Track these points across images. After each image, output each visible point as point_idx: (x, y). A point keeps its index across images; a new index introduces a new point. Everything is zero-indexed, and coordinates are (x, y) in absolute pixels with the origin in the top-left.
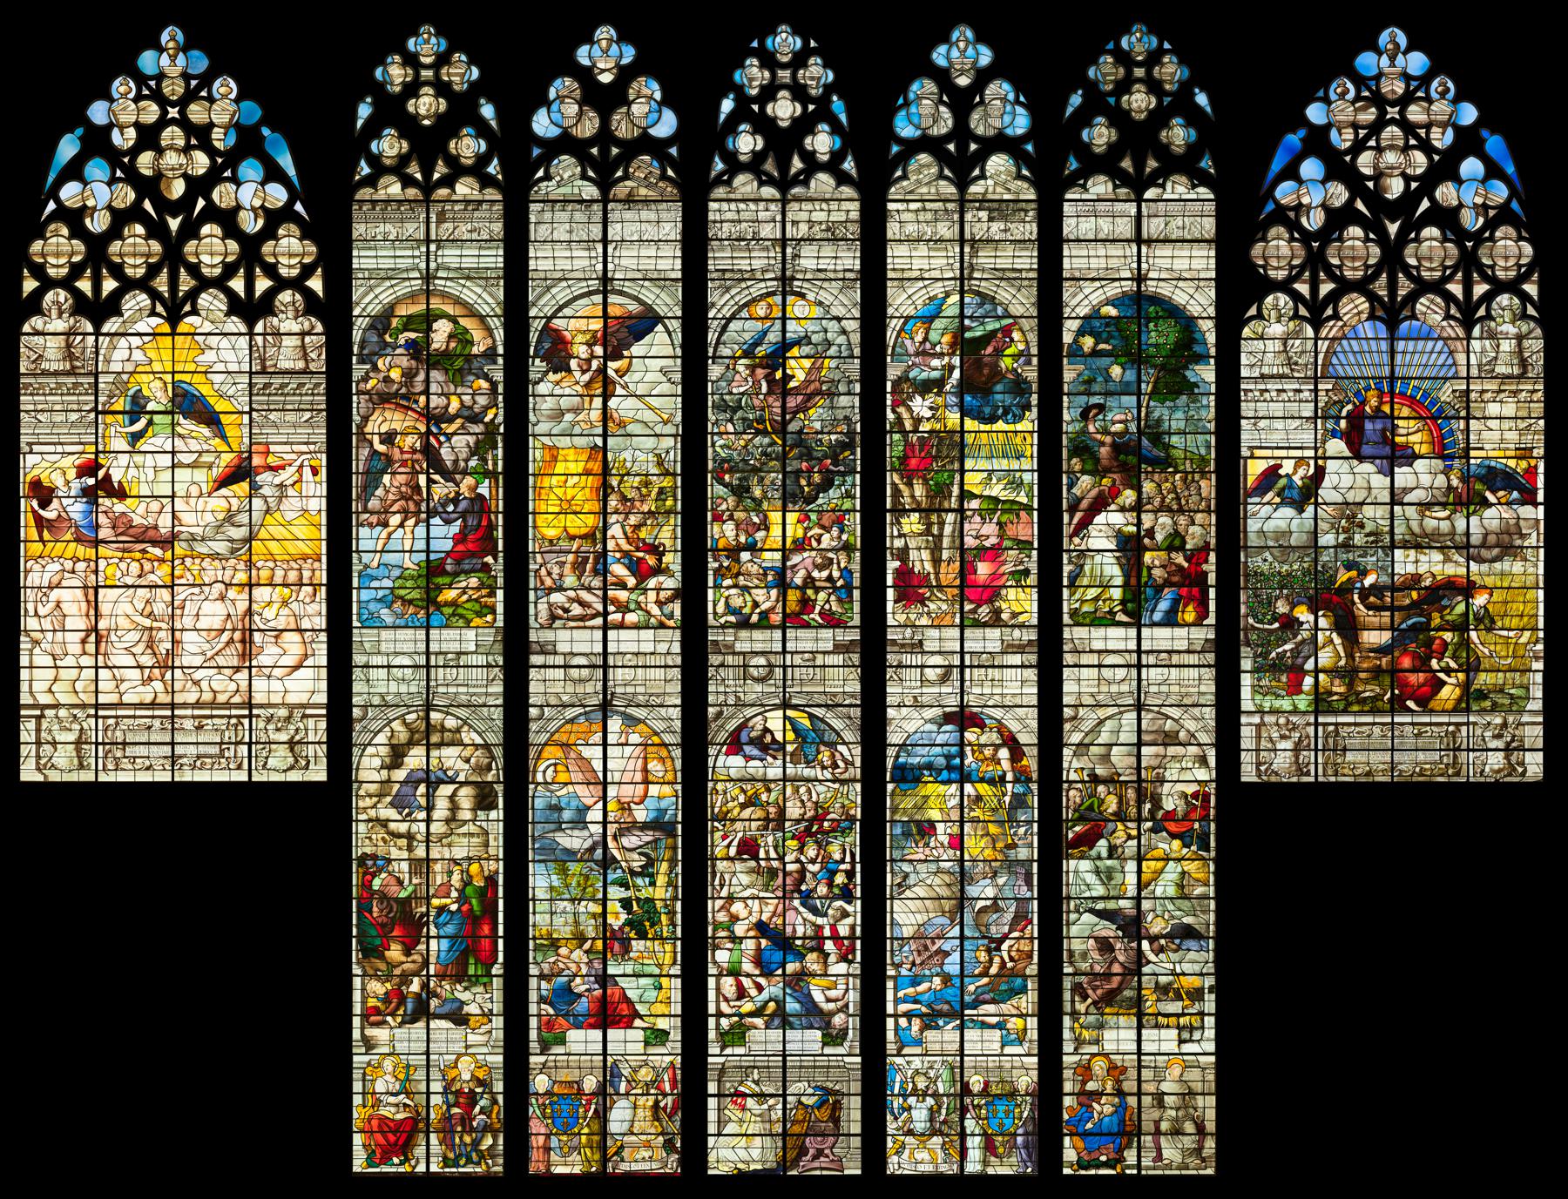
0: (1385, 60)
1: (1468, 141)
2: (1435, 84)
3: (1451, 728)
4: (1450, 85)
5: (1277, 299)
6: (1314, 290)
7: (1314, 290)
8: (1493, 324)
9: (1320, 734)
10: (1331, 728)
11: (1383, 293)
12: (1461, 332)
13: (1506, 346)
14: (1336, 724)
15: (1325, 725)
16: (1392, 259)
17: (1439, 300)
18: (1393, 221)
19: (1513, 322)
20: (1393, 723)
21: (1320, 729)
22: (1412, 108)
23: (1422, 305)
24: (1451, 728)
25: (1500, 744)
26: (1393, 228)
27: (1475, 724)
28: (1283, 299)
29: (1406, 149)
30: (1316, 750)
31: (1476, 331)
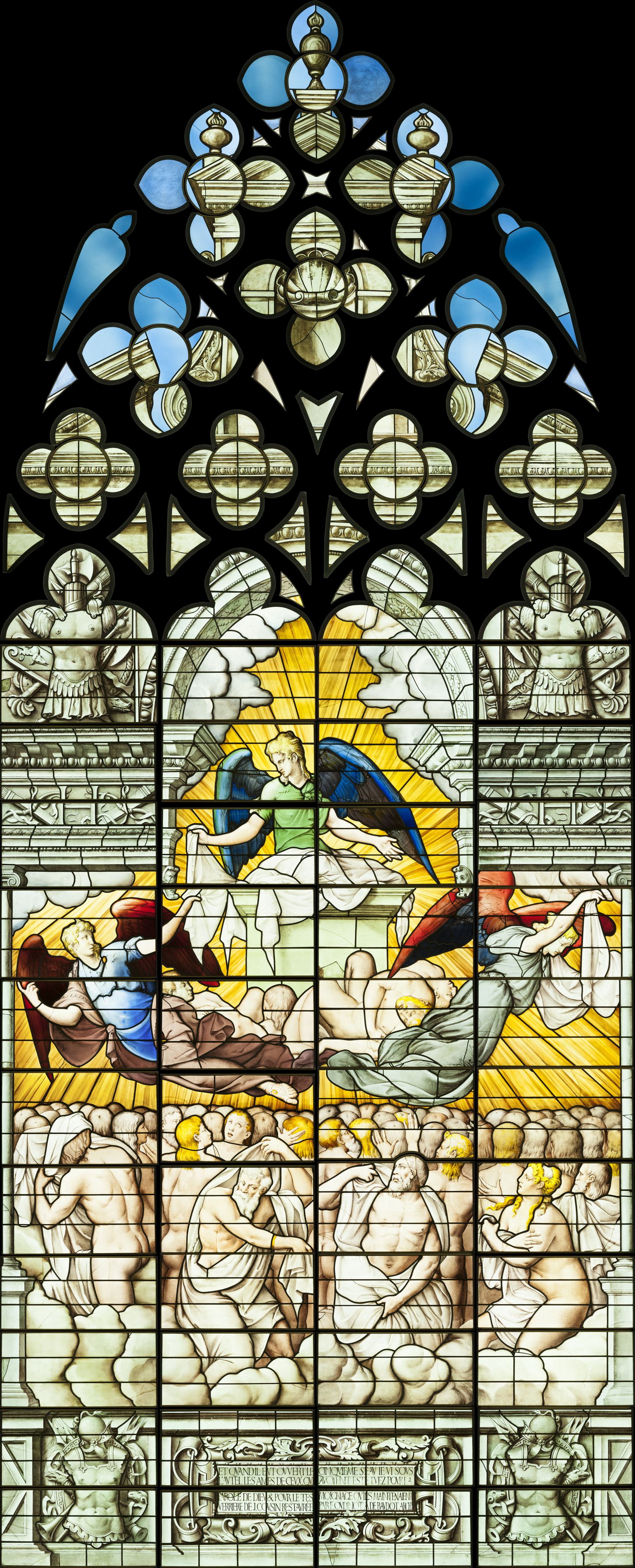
0: (299, 76)
1: (472, 247)
2: (407, 125)
3: (441, 1442)
4: (439, 126)
5: (79, 561)
6: (160, 544)
7: (160, 544)
8: (527, 612)
9: (166, 1454)
10: (189, 1443)
11: (297, 549)
12: (460, 631)
13: (552, 658)
14: (200, 1434)
15: (176, 1434)
16: (317, 483)
17: (417, 564)
18: (319, 400)
19: (569, 609)
20: (316, 1432)
21: (167, 1442)
22: (357, 173)
23: (381, 571)
24: (441, 1442)
25: (544, 1475)
26: (318, 414)
27: (492, 1432)
28: (88, 561)
29: (344, 261)
30: (159, 1489)
31: (493, 629)
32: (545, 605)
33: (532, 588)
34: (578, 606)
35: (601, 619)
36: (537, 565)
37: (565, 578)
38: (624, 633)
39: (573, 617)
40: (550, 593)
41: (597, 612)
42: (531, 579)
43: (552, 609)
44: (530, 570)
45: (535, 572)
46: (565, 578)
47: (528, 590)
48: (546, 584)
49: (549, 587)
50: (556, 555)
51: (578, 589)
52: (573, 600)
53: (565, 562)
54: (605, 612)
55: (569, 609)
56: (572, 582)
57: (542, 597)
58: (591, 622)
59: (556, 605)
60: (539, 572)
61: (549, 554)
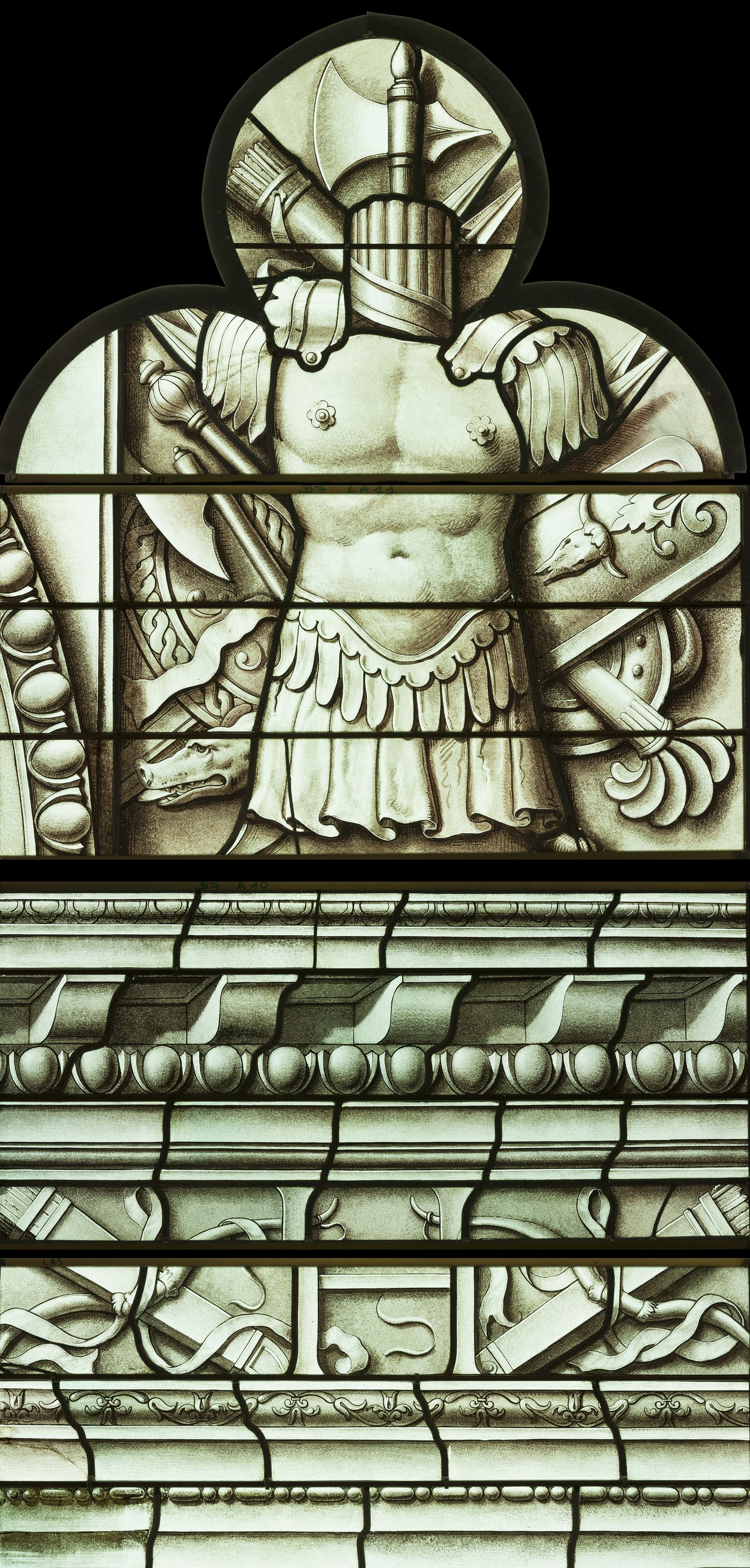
13: (362, 555)
19: (441, 326)
32: (326, 303)
33: (259, 220)
34: (485, 310)
35: (598, 375)
36: (284, 107)
37: (423, 172)
38: (712, 442)
39: (464, 364)
40: (349, 247)
41: (578, 339)
42: (253, 173)
43: (357, 324)
44: (247, 134)
45: (272, 143)
46: (423, 172)
47: (240, 232)
48: (328, 199)
49: (344, 217)
50: (380, 58)
51: (484, 227)
52: (460, 280)
53: (423, 91)
54: (618, 338)
55: (441, 326)
56: (456, 191)
57: (307, 262)
58: (553, 388)
59: (379, 304)
60: (294, 143)
61: (343, 53)
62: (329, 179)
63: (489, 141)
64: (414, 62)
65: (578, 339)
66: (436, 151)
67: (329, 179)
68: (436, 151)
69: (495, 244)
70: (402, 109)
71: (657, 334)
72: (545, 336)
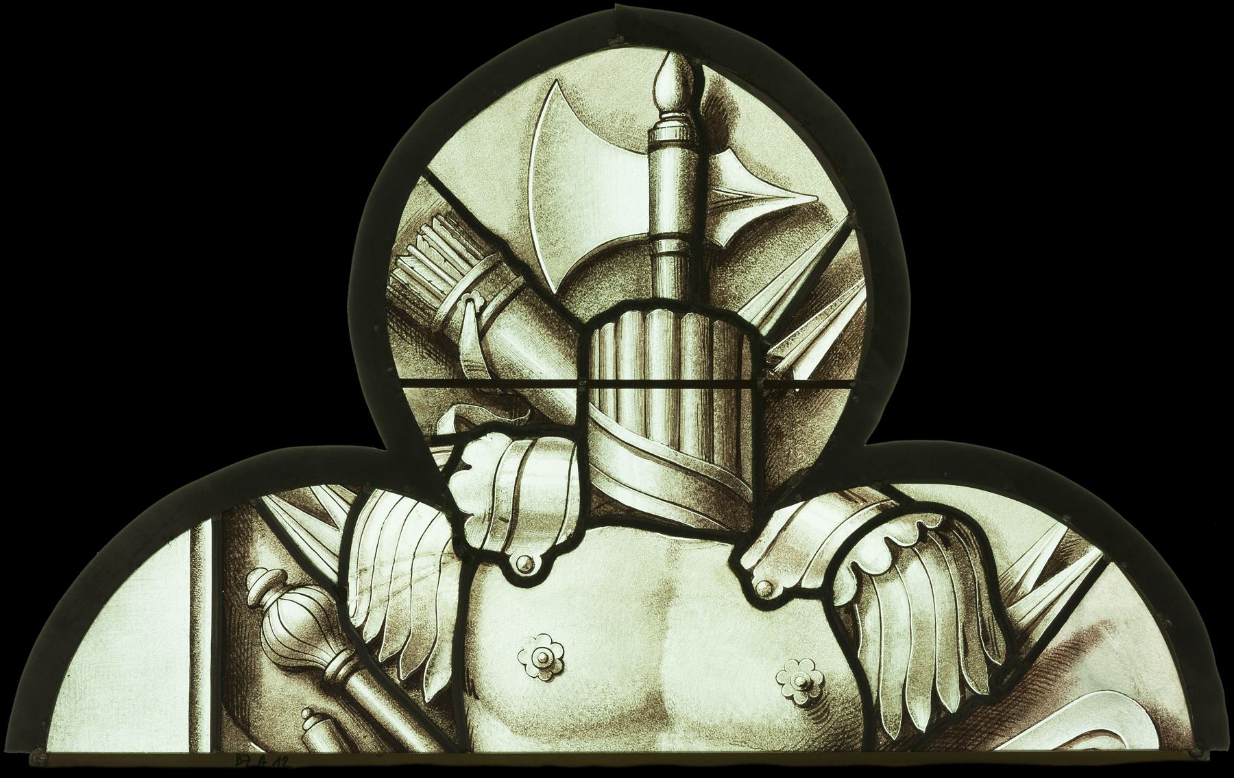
8: (397, 546)
19: (736, 512)
32: (549, 474)
33: (441, 342)
34: (806, 487)
35: (990, 592)
36: (480, 159)
37: (705, 265)
38: (1174, 702)
40: (585, 384)
41: (956, 534)
42: (430, 266)
43: (598, 510)
46: (705, 265)
47: (409, 362)
48: (553, 308)
49: (580, 338)
50: (634, 79)
51: (804, 354)
52: (767, 439)
53: (705, 132)
54: (1023, 532)
55: (736, 512)
56: (759, 295)
57: (517, 408)
59: (634, 478)
61: (575, 72)
62: (553, 274)
63: (812, 213)
64: (691, 85)
65: (956, 534)
66: (727, 229)
67: (553, 274)
68: (727, 229)
69: (822, 381)
70: (672, 162)
71: (1085, 526)
72: (903, 530)
